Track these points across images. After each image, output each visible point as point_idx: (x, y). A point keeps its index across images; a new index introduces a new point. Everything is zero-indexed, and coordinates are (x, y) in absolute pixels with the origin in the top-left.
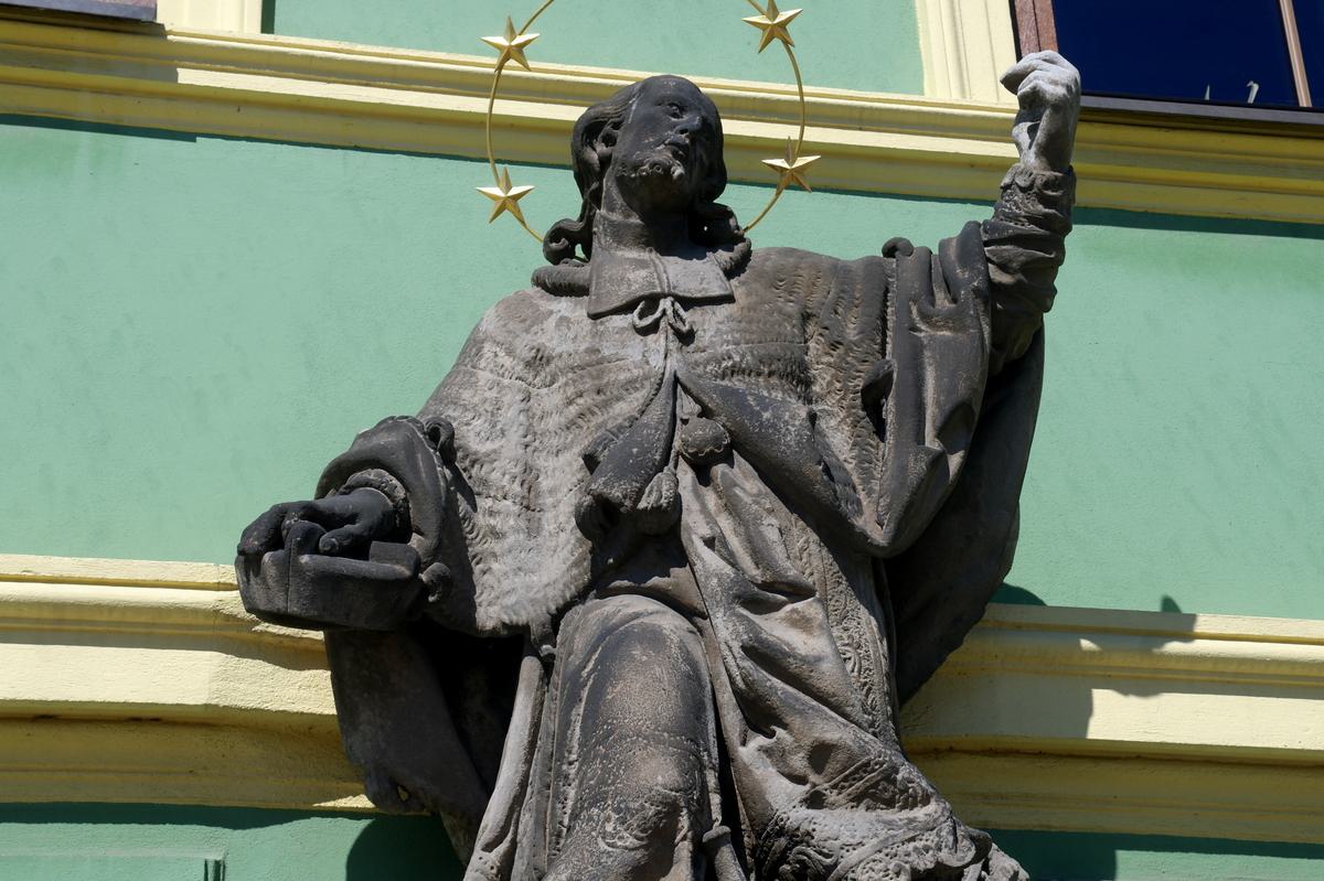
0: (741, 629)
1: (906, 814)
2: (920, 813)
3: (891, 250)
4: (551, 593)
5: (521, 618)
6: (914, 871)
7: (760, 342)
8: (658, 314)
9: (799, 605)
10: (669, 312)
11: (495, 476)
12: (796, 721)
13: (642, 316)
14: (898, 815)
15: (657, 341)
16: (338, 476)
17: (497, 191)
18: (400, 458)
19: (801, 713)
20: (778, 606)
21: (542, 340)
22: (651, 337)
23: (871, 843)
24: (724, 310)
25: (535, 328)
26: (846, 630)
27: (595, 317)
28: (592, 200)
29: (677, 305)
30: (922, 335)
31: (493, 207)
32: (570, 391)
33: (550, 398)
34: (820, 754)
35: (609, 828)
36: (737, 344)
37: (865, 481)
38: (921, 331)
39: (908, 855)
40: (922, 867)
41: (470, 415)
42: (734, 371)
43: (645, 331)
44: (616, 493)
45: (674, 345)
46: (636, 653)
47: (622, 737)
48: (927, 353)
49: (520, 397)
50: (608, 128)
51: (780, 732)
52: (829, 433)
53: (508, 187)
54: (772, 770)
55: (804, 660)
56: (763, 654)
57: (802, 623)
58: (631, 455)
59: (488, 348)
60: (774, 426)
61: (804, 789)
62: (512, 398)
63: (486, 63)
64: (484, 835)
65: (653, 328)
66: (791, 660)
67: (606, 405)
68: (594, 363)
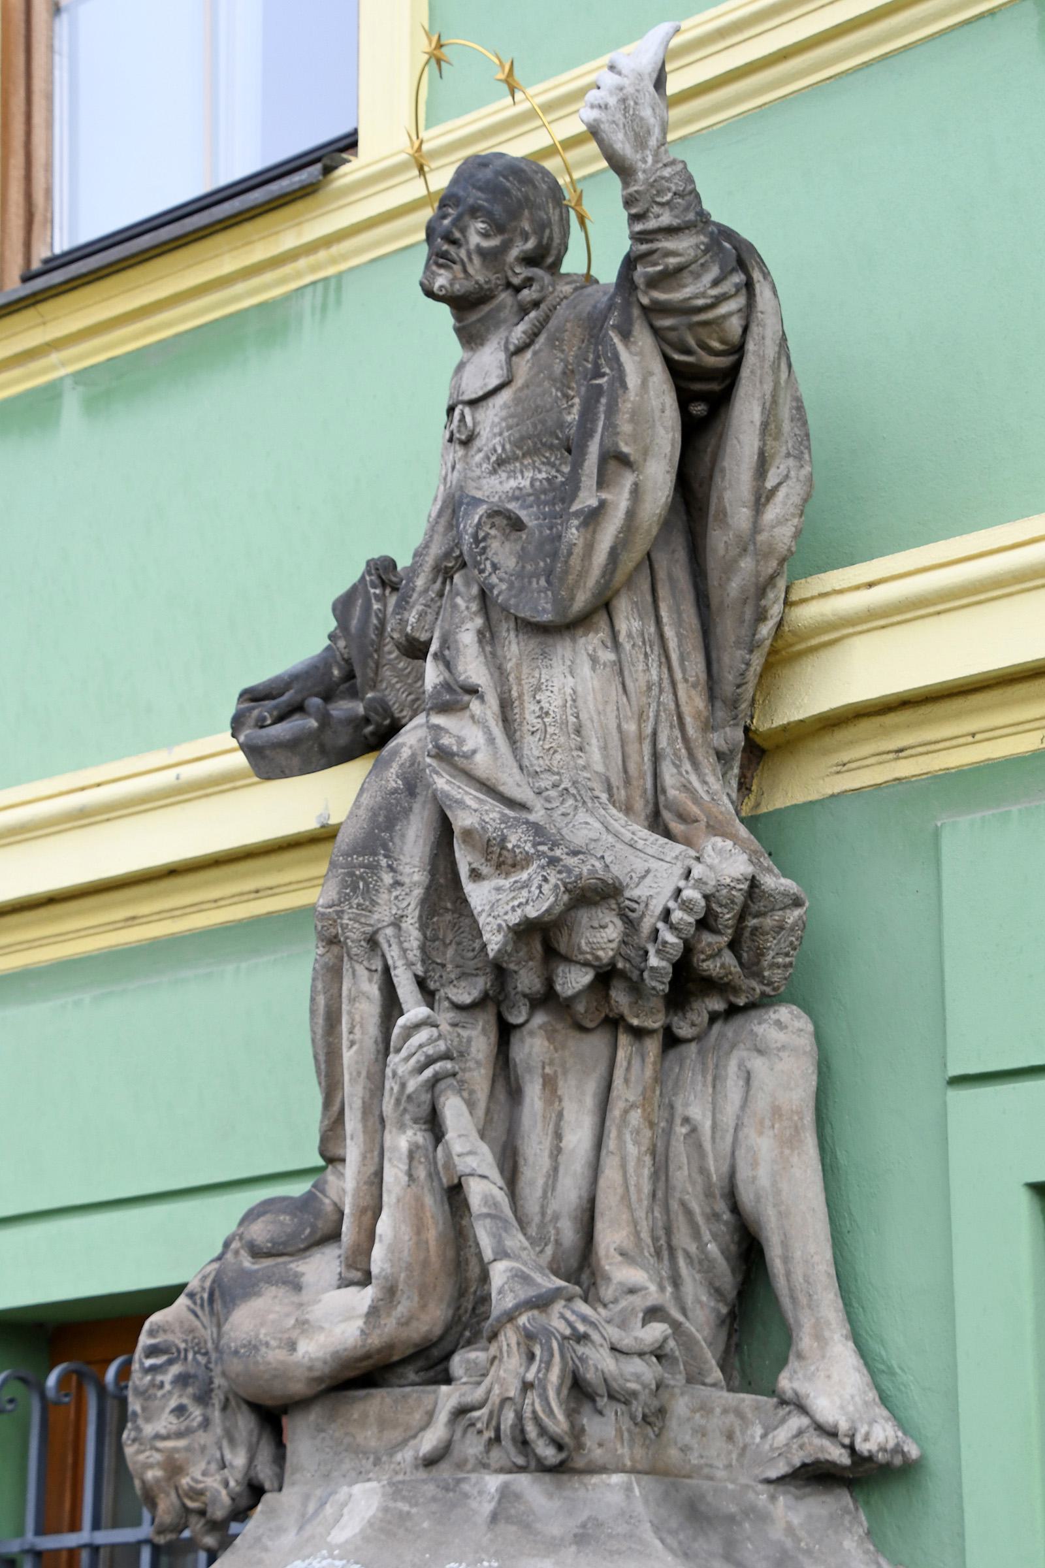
7: (518, 425)
24: (505, 396)
26: (539, 702)
29: (467, 411)
30: (605, 379)
36: (501, 434)
38: (603, 375)
39: (506, 913)
42: (501, 463)
45: (461, 452)
66: (456, 758)
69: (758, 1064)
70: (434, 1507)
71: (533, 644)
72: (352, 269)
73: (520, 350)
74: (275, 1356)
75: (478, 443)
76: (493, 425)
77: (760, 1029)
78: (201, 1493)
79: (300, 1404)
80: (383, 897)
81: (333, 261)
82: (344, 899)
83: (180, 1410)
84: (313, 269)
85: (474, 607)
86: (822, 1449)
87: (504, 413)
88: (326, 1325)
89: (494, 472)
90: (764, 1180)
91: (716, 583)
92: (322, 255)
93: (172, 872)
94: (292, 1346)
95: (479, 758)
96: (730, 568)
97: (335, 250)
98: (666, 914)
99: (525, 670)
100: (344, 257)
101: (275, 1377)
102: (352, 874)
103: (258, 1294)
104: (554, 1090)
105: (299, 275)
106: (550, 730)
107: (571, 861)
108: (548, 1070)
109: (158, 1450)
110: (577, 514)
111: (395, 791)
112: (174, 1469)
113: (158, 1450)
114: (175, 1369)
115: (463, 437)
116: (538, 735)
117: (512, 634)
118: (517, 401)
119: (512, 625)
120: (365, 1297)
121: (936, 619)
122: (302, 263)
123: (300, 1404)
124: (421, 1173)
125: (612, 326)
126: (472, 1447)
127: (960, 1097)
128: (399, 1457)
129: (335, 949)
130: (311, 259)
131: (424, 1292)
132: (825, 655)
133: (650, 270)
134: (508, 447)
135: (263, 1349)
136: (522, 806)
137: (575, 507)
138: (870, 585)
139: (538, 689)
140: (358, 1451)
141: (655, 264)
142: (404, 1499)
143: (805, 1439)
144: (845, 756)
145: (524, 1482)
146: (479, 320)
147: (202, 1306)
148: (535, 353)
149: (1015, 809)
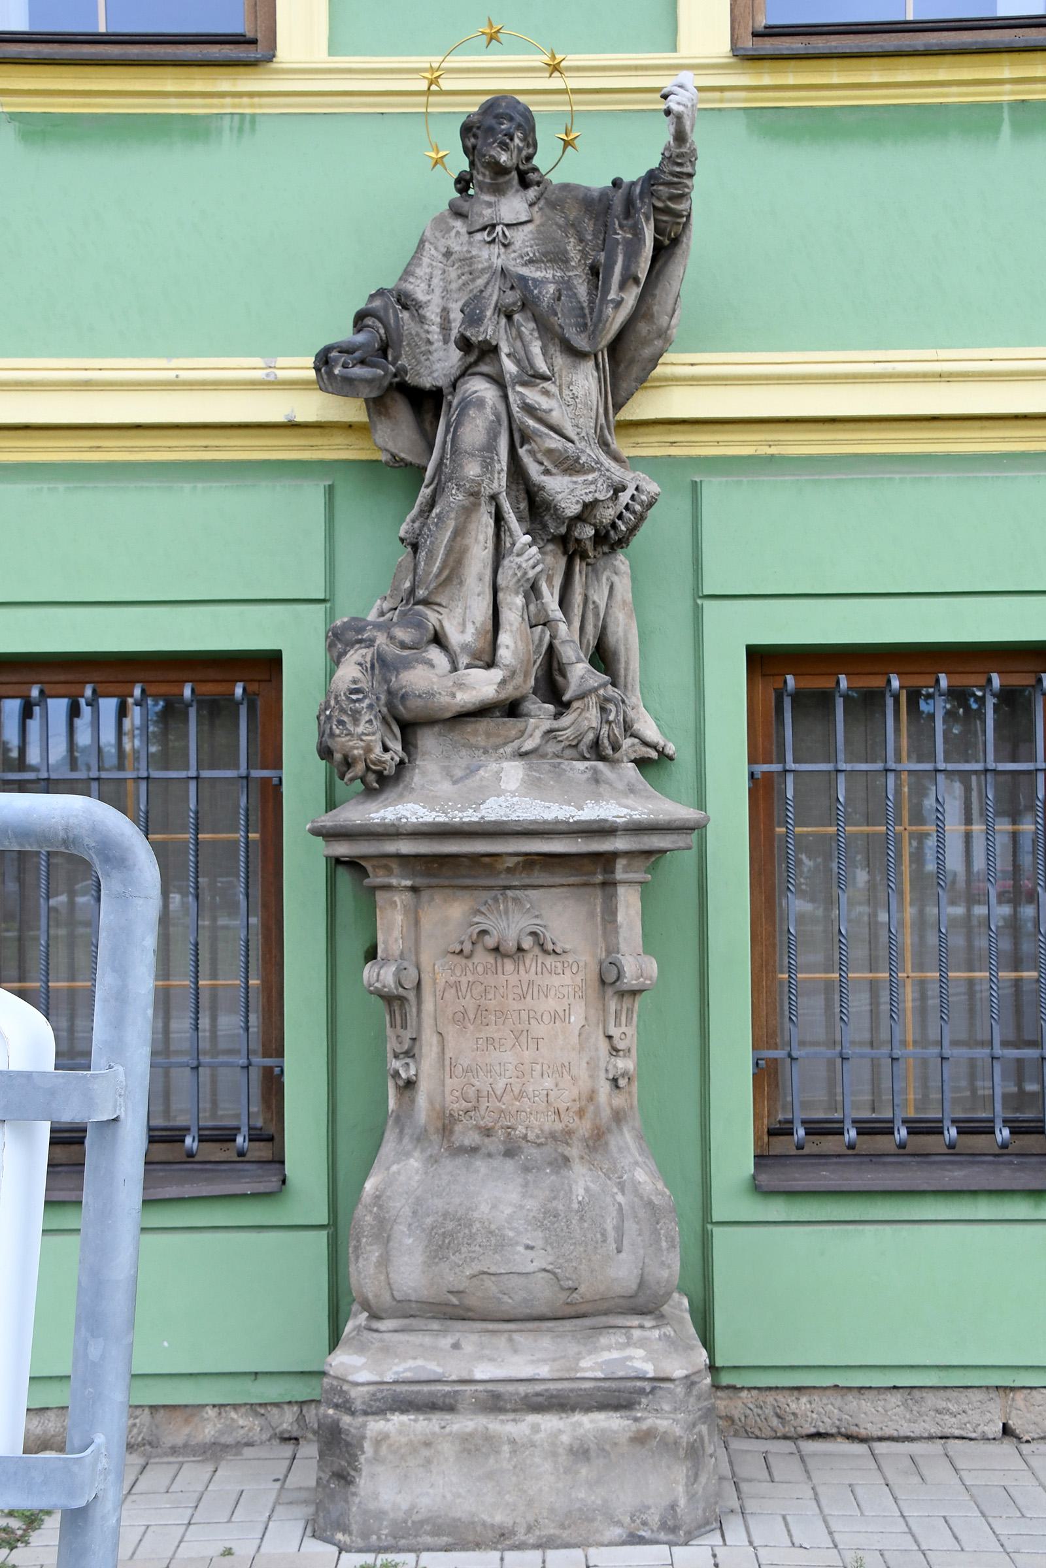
0: (517, 398)
1: (585, 477)
2: (590, 477)
3: (617, 183)
4: (453, 371)
5: (440, 383)
6: (584, 502)
8: (495, 235)
9: (546, 385)
10: (500, 234)
11: (428, 314)
12: (538, 439)
13: (489, 234)
14: (580, 479)
15: (496, 249)
16: (360, 319)
17: (433, 155)
18: (382, 314)
19: (540, 436)
20: (537, 385)
21: (449, 242)
22: (492, 246)
23: (567, 491)
25: (447, 236)
27: (470, 233)
28: (472, 164)
29: (505, 229)
30: (619, 237)
31: (433, 162)
32: (460, 272)
33: (453, 273)
34: (549, 452)
35: (454, 492)
36: (531, 247)
37: (591, 313)
38: (618, 234)
40: (587, 501)
41: (419, 281)
42: (531, 261)
43: (489, 243)
44: (468, 334)
45: (502, 250)
46: (471, 412)
47: (461, 453)
48: (620, 247)
49: (440, 272)
50: (474, 130)
51: (533, 444)
52: (578, 287)
53: (438, 152)
54: (531, 459)
55: (544, 411)
56: (529, 409)
57: (546, 393)
58: (476, 314)
59: (427, 244)
60: (538, 298)
61: (543, 468)
62: (438, 272)
63: (423, 86)
64: (426, 482)
65: (493, 241)
67: (473, 280)
68: (468, 260)
69: (615, 579)
70: (551, 775)
71: (569, 361)
72: (264, 114)
73: (531, 205)
74: (445, 699)
75: (512, 248)
76: (524, 241)
77: (617, 563)
78: (384, 762)
79: (431, 722)
80: (496, 475)
81: (252, 106)
82: (484, 474)
83: (370, 722)
84: (234, 106)
85: (536, 334)
86: (647, 752)
87: (530, 236)
88: (477, 687)
89: (526, 264)
90: (621, 634)
91: (632, 348)
92: (245, 100)
93: (138, 427)
94: (454, 696)
95: (554, 414)
96: (645, 342)
97: (256, 100)
98: (627, 507)
99: (564, 373)
100: (261, 106)
101: (441, 709)
102: (485, 462)
103: (413, 667)
104: (551, 582)
105: (223, 106)
106: (579, 406)
107: (608, 474)
108: (550, 572)
109: (362, 740)
110: (612, 301)
111: (493, 421)
112: (368, 749)
113: (362, 740)
114: (367, 702)
115: (506, 243)
116: (572, 407)
117: (558, 354)
118: (539, 232)
119: (558, 349)
120: (496, 674)
121: (723, 387)
122: (228, 100)
123: (431, 722)
124: (526, 617)
125: (644, 213)
126: (552, 748)
127: (708, 605)
128: (502, 750)
129: (472, 499)
130: (237, 100)
131: (526, 675)
132: (654, 391)
133: (675, 191)
134: (537, 254)
135: (438, 696)
136: (572, 442)
137: (609, 298)
138: (692, 365)
139: (571, 383)
140: (471, 747)
141: (676, 189)
142: (535, 771)
143: (636, 748)
144: (640, 440)
145: (600, 765)
146: (505, 183)
147: (367, 671)
148: (540, 209)
149: (745, 480)
